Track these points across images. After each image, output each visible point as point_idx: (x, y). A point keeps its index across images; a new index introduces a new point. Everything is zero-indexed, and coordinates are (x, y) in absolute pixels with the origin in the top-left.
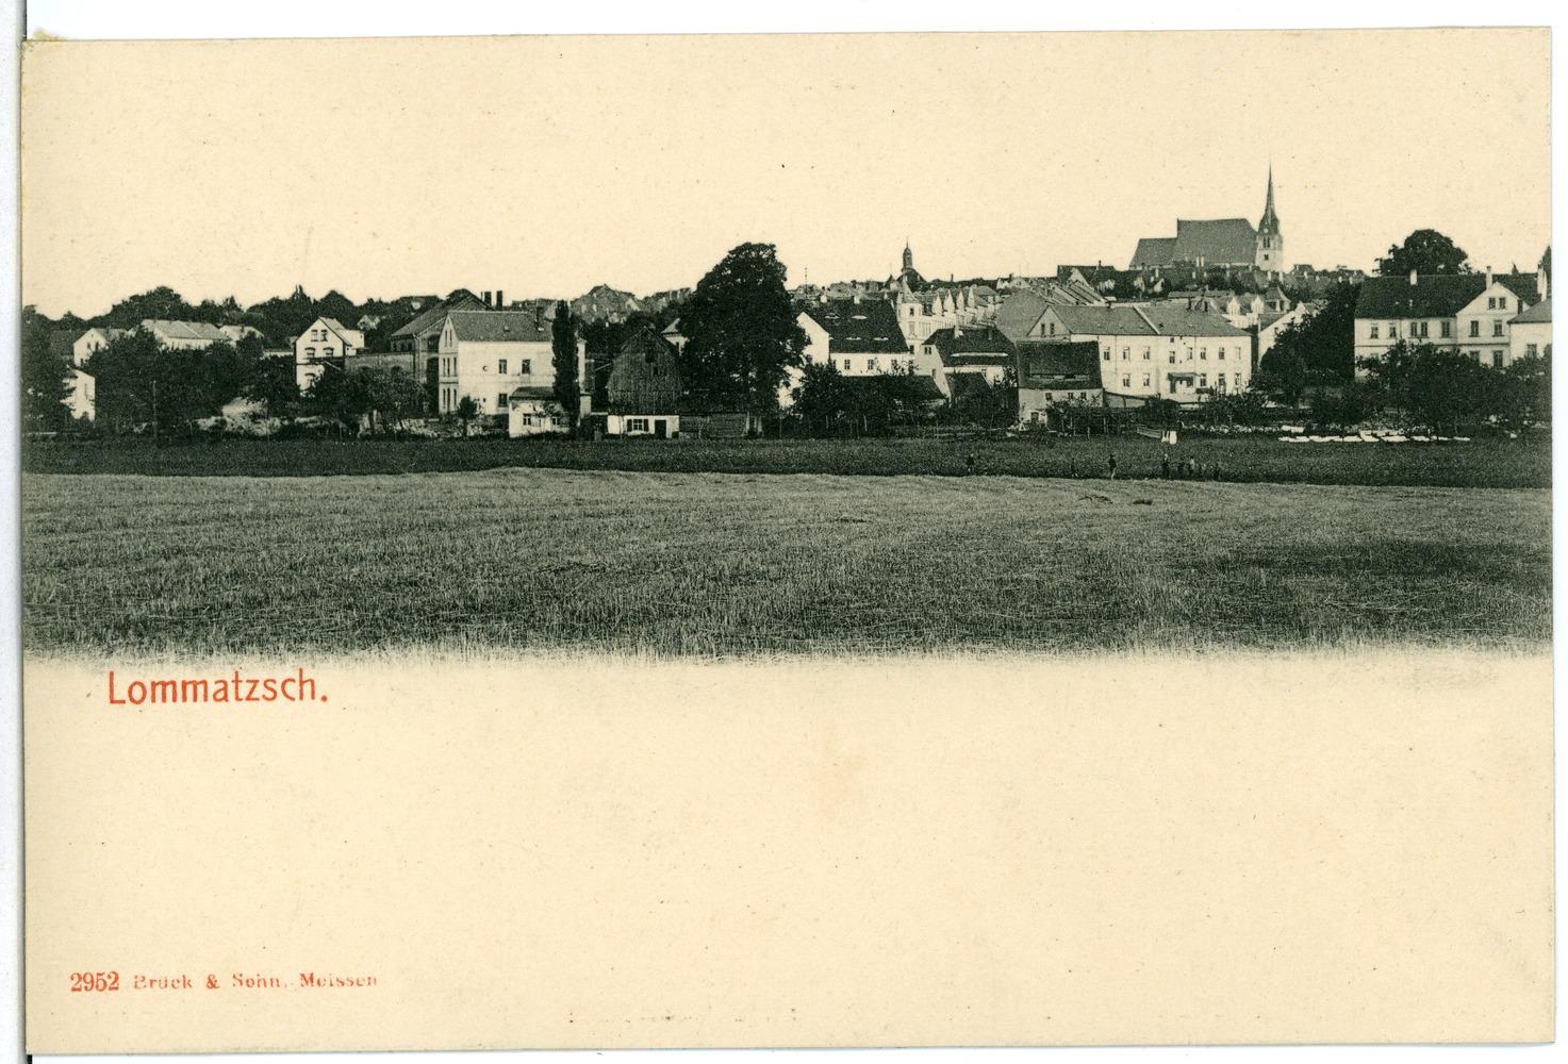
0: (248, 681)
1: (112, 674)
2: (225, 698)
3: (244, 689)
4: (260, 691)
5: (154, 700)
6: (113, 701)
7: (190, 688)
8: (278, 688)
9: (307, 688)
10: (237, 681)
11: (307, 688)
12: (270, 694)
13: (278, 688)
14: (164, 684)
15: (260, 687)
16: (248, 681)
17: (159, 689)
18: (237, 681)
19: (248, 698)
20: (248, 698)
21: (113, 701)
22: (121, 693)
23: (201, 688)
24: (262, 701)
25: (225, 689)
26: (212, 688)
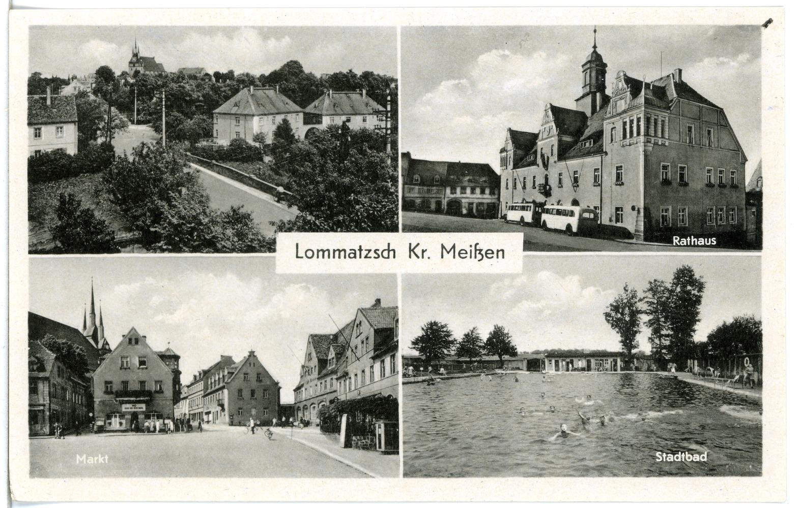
0: (366, 250)
1: (297, 245)
2: (355, 257)
3: (364, 253)
4: (372, 254)
5: (318, 257)
6: (297, 257)
7: (337, 253)
8: (379, 253)
9: (392, 253)
10: (360, 250)
11: (392, 253)
12: (377, 256)
13: (380, 254)
14: (340, 251)
15: (372, 252)
16: (366, 250)
17: (337, 253)
18: (360, 250)
19: (366, 257)
20: (366, 257)
21: (297, 257)
22: (301, 253)
23: (342, 253)
24: (372, 258)
25: (355, 254)
26: (348, 252)
